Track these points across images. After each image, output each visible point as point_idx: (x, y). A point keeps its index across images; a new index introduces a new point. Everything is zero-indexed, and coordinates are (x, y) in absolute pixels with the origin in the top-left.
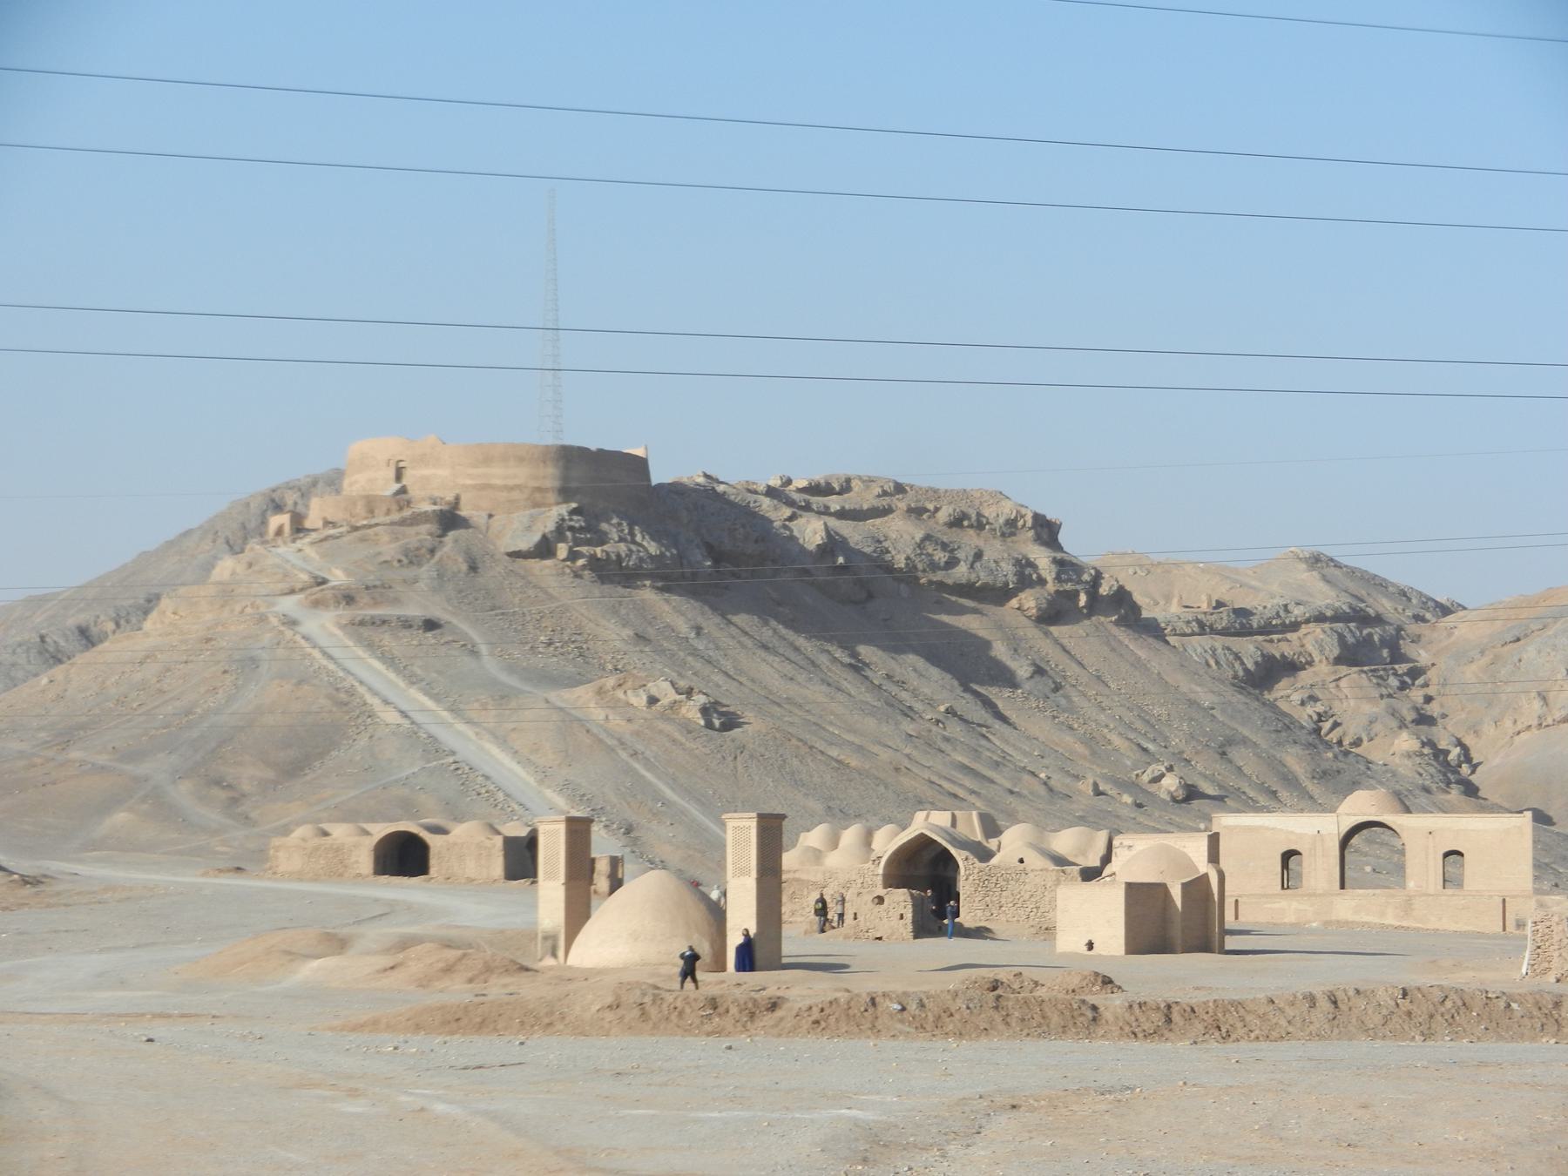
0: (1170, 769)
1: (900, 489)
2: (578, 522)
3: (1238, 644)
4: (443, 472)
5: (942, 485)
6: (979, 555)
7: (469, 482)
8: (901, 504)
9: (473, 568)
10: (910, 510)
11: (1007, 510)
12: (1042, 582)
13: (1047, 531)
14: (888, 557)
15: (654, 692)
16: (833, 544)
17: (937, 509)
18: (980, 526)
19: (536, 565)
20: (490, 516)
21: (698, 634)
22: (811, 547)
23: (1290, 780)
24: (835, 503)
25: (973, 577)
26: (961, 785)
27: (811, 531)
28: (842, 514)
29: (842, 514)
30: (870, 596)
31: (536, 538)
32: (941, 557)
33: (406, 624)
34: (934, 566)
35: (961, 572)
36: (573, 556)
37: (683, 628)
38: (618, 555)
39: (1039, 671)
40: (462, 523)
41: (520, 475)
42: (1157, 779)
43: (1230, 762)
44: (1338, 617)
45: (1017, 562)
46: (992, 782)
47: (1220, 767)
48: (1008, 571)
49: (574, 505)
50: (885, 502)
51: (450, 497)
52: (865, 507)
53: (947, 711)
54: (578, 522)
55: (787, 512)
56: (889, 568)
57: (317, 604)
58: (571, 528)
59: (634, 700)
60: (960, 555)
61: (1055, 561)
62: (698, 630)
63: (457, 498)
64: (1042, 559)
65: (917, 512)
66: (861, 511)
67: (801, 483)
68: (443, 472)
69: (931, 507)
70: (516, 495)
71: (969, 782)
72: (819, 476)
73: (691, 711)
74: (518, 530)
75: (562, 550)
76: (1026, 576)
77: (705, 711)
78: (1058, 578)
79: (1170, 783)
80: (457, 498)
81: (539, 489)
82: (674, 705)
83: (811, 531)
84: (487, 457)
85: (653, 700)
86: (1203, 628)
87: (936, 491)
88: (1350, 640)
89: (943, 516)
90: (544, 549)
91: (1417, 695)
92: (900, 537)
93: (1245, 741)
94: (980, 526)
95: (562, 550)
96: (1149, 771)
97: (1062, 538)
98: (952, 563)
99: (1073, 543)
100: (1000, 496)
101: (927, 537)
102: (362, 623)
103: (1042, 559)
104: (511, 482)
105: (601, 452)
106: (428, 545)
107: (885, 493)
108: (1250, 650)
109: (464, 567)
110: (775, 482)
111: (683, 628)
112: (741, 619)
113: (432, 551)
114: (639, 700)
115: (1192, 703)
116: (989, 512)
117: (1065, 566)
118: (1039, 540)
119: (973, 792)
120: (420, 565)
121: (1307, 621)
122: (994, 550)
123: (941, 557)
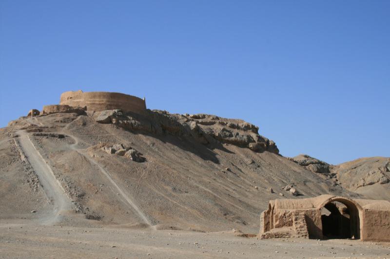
0: (292, 187)
1: (217, 118)
2: (120, 113)
4: (82, 100)
5: (228, 118)
6: (238, 134)
7: (89, 103)
8: (218, 121)
9: (84, 124)
10: (220, 123)
11: (245, 123)
12: (254, 141)
13: (255, 130)
14: (213, 133)
15: (114, 147)
16: (197, 129)
17: (227, 123)
18: (238, 128)
19: (105, 125)
20: (94, 112)
21: (153, 145)
22: (192, 129)
24: (200, 121)
25: (236, 139)
26: (229, 187)
27: (193, 125)
28: (202, 123)
29: (202, 123)
31: (107, 117)
32: (227, 133)
33: (53, 136)
34: (226, 136)
35: (233, 138)
36: (117, 124)
37: (148, 143)
38: (132, 123)
39: (253, 162)
40: (85, 114)
41: (105, 100)
42: (288, 190)
43: (307, 186)
44: (316, 163)
45: (248, 136)
46: (241, 187)
47: (304, 188)
48: (245, 137)
50: (214, 121)
51: (83, 107)
52: (208, 121)
53: (228, 170)
54: (120, 113)
55: (186, 120)
56: (214, 136)
59: (107, 151)
60: (233, 134)
61: (257, 136)
62: (153, 144)
63: (86, 107)
64: (254, 135)
65: (222, 124)
66: (207, 122)
67: (191, 115)
68: (82, 100)
69: (225, 123)
70: (102, 106)
71: (234, 187)
72: (196, 114)
74: (102, 115)
76: (250, 139)
77: (133, 155)
78: (258, 141)
79: (292, 190)
80: (86, 107)
81: (110, 105)
82: (122, 154)
83: (193, 125)
84: (94, 95)
85: (113, 151)
87: (227, 119)
88: (319, 167)
89: (228, 125)
90: (109, 121)
91: (334, 179)
92: (217, 129)
93: (310, 181)
96: (286, 187)
97: (259, 132)
98: (231, 136)
99: (261, 133)
100: (242, 121)
101: (224, 130)
103: (254, 135)
104: (101, 103)
105: (129, 96)
106: (72, 118)
107: (213, 119)
109: (82, 124)
110: (185, 115)
111: (148, 143)
112: (167, 143)
113: (73, 119)
114: (109, 151)
115: (295, 172)
116: (240, 125)
117: (260, 138)
118: (253, 131)
119: (234, 190)
120: (68, 123)
121: (310, 163)
122: (241, 133)
123: (227, 133)
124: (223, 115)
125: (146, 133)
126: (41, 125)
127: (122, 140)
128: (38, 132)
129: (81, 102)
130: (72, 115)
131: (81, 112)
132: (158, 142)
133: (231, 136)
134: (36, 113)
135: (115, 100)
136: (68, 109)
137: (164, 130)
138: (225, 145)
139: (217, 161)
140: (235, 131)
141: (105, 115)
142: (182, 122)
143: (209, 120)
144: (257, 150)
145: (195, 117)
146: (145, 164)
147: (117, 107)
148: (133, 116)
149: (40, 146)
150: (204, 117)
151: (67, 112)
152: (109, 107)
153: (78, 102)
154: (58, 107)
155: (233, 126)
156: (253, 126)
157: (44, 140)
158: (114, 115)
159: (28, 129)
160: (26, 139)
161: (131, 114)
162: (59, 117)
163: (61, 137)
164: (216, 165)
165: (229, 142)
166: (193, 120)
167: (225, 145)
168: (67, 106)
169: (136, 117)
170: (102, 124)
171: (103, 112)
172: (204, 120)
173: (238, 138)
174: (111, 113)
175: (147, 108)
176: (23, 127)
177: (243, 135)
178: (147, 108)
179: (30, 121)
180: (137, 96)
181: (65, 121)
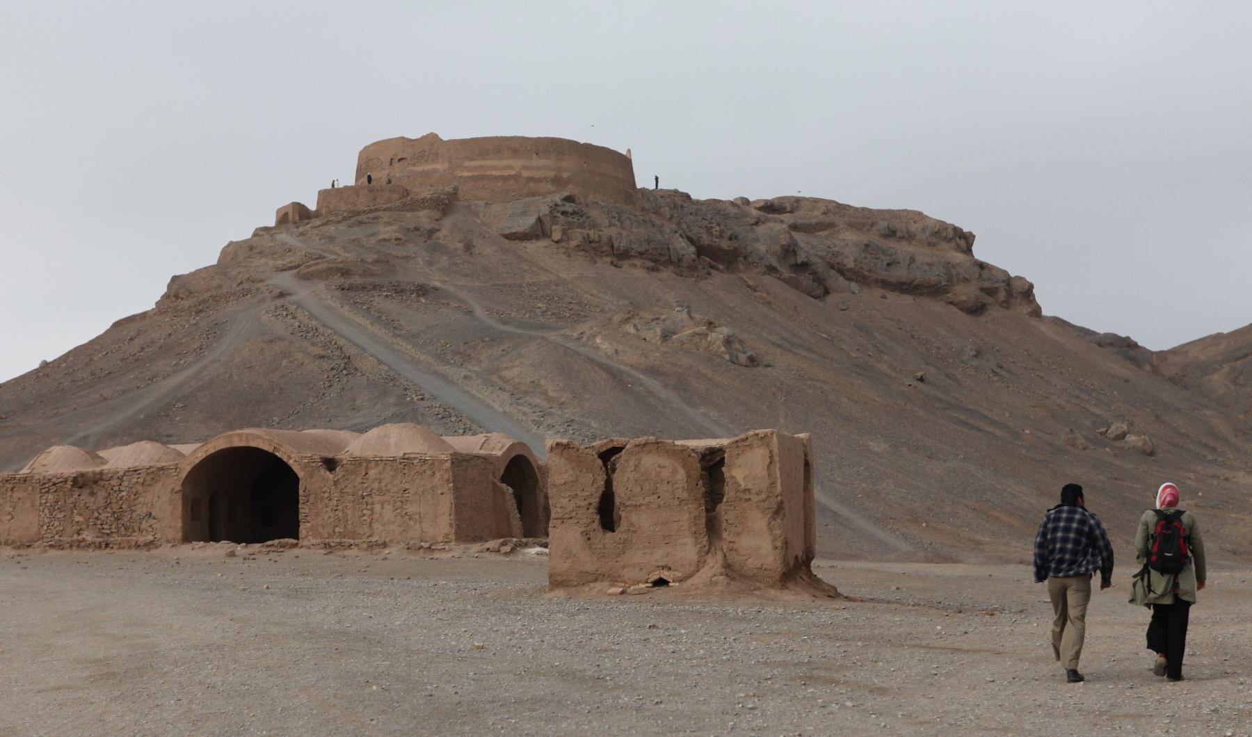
4: (440, 167)
6: (912, 259)
9: (469, 247)
13: (964, 240)
14: (839, 259)
18: (910, 237)
30: (827, 292)
31: (532, 220)
38: (610, 239)
49: (566, 194)
51: (449, 189)
57: (307, 277)
58: (564, 213)
59: (644, 334)
68: (440, 167)
85: (666, 336)
90: (539, 232)
92: (848, 242)
94: (910, 237)
99: (980, 252)
102: (350, 288)
105: (588, 147)
106: (429, 227)
109: (460, 246)
116: (914, 227)
122: (924, 255)
128: (353, 282)
130: (424, 218)
140: (903, 249)
141: (524, 213)
143: (817, 216)
144: (976, 310)
150: (796, 203)
151: (404, 208)
153: (426, 174)
155: (891, 234)
156: (957, 230)
159: (304, 270)
163: (422, 290)
170: (524, 244)
172: (800, 217)
175: (639, 186)
176: (280, 262)
178: (639, 186)
180: (612, 148)
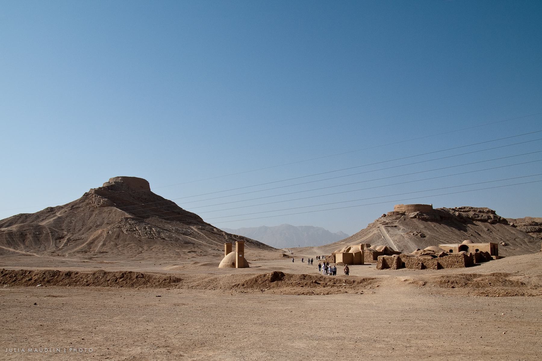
1: (472, 208)
3: (535, 227)
11: (487, 210)
13: (493, 212)
18: (483, 212)
23: (525, 243)
24: (462, 210)
28: (463, 212)
29: (463, 212)
33: (392, 226)
35: (479, 218)
36: (419, 218)
37: (433, 225)
39: (488, 230)
56: (469, 218)
64: (492, 216)
65: (475, 211)
73: (419, 235)
74: (412, 215)
75: (417, 217)
76: (489, 218)
79: (503, 244)
82: (417, 235)
84: (408, 206)
85: (414, 234)
86: (530, 225)
90: (415, 217)
92: (471, 214)
94: (483, 212)
95: (417, 217)
98: (478, 217)
100: (486, 208)
103: (492, 216)
108: (537, 227)
114: (412, 234)
117: (496, 217)
122: (484, 215)
124: (475, 206)
125: (432, 220)
126: (387, 221)
127: (421, 225)
129: (403, 209)
130: (399, 216)
131: (403, 214)
132: (437, 225)
133: (478, 217)
134: (385, 215)
135: (417, 207)
136: (398, 213)
137: (441, 217)
138: (474, 222)
139: (466, 231)
140: (481, 214)
142: (451, 212)
143: (467, 209)
144: (493, 223)
145: (460, 208)
146: (426, 238)
147: (418, 210)
148: (427, 214)
149: (388, 231)
150: (465, 208)
152: (415, 211)
154: (394, 212)
155: (480, 212)
157: (389, 229)
158: (417, 214)
160: (383, 228)
161: (425, 213)
162: (394, 218)
163: (396, 226)
164: (465, 233)
165: (477, 220)
166: (458, 211)
167: (474, 222)
168: (398, 212)
169: (427, 214)
171: (412, 213)
173: (482, 218)
174: (416, 213)
177: (485, 216)
179: (384, 219)
181: (397, 219)
